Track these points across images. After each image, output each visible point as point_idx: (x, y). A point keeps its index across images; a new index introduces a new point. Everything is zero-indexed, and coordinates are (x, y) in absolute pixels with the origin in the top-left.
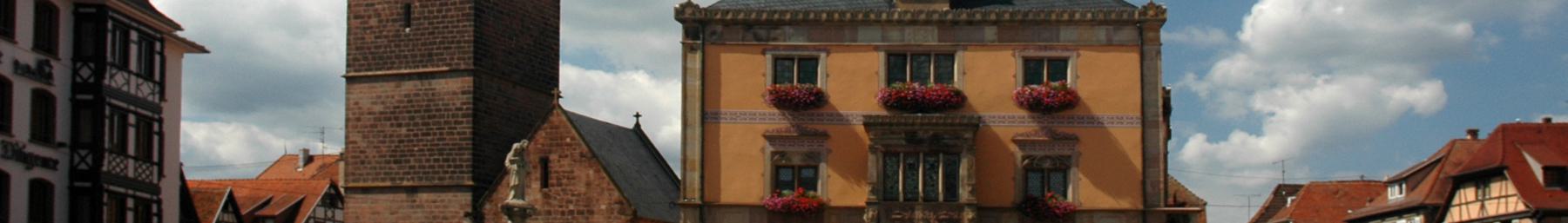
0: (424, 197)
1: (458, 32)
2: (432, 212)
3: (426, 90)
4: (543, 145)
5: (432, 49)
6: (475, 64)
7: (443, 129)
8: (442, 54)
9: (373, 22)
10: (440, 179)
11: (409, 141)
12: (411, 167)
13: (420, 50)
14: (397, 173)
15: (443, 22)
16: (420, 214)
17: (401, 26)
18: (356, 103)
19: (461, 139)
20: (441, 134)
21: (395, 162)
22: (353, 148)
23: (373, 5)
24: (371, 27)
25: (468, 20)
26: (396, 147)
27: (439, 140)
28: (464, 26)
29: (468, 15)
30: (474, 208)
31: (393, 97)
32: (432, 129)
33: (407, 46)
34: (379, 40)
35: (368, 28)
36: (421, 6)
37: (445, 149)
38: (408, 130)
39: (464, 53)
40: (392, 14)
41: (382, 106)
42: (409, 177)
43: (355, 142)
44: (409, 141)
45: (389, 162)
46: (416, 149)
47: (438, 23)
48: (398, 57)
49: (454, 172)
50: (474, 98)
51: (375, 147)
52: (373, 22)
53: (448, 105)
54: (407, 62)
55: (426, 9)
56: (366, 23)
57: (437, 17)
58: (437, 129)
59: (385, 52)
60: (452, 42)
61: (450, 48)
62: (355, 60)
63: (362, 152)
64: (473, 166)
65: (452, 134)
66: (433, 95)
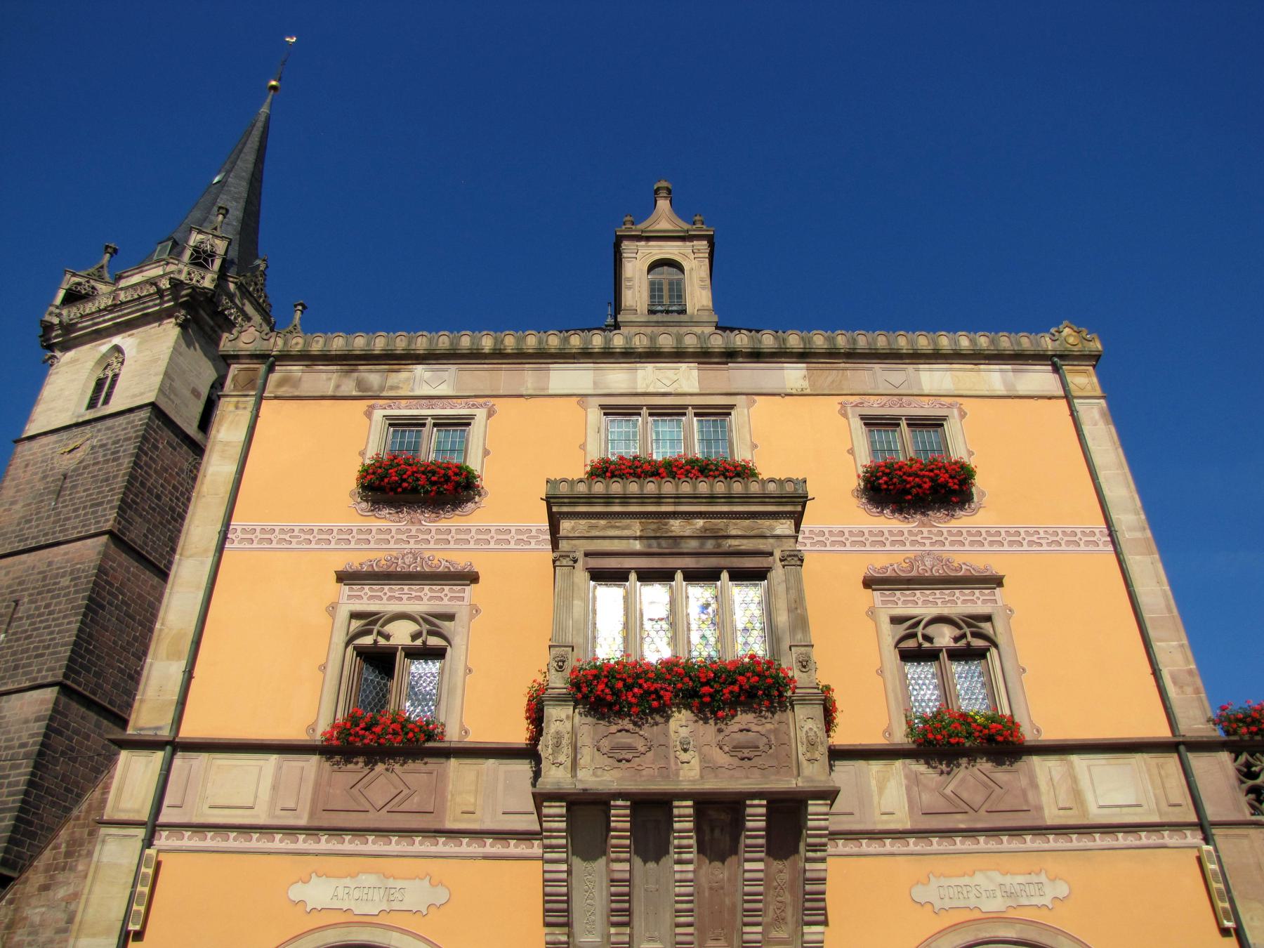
6: (66, 676)
8: (30, 665)
25: (77, 614)
28: (69, 623)
29: (79, 607)
36: (31, 602)
39: (58, 660)
50: (48, 727)
55: (33, 606)
60: (48, 647)
61: (42, 655)
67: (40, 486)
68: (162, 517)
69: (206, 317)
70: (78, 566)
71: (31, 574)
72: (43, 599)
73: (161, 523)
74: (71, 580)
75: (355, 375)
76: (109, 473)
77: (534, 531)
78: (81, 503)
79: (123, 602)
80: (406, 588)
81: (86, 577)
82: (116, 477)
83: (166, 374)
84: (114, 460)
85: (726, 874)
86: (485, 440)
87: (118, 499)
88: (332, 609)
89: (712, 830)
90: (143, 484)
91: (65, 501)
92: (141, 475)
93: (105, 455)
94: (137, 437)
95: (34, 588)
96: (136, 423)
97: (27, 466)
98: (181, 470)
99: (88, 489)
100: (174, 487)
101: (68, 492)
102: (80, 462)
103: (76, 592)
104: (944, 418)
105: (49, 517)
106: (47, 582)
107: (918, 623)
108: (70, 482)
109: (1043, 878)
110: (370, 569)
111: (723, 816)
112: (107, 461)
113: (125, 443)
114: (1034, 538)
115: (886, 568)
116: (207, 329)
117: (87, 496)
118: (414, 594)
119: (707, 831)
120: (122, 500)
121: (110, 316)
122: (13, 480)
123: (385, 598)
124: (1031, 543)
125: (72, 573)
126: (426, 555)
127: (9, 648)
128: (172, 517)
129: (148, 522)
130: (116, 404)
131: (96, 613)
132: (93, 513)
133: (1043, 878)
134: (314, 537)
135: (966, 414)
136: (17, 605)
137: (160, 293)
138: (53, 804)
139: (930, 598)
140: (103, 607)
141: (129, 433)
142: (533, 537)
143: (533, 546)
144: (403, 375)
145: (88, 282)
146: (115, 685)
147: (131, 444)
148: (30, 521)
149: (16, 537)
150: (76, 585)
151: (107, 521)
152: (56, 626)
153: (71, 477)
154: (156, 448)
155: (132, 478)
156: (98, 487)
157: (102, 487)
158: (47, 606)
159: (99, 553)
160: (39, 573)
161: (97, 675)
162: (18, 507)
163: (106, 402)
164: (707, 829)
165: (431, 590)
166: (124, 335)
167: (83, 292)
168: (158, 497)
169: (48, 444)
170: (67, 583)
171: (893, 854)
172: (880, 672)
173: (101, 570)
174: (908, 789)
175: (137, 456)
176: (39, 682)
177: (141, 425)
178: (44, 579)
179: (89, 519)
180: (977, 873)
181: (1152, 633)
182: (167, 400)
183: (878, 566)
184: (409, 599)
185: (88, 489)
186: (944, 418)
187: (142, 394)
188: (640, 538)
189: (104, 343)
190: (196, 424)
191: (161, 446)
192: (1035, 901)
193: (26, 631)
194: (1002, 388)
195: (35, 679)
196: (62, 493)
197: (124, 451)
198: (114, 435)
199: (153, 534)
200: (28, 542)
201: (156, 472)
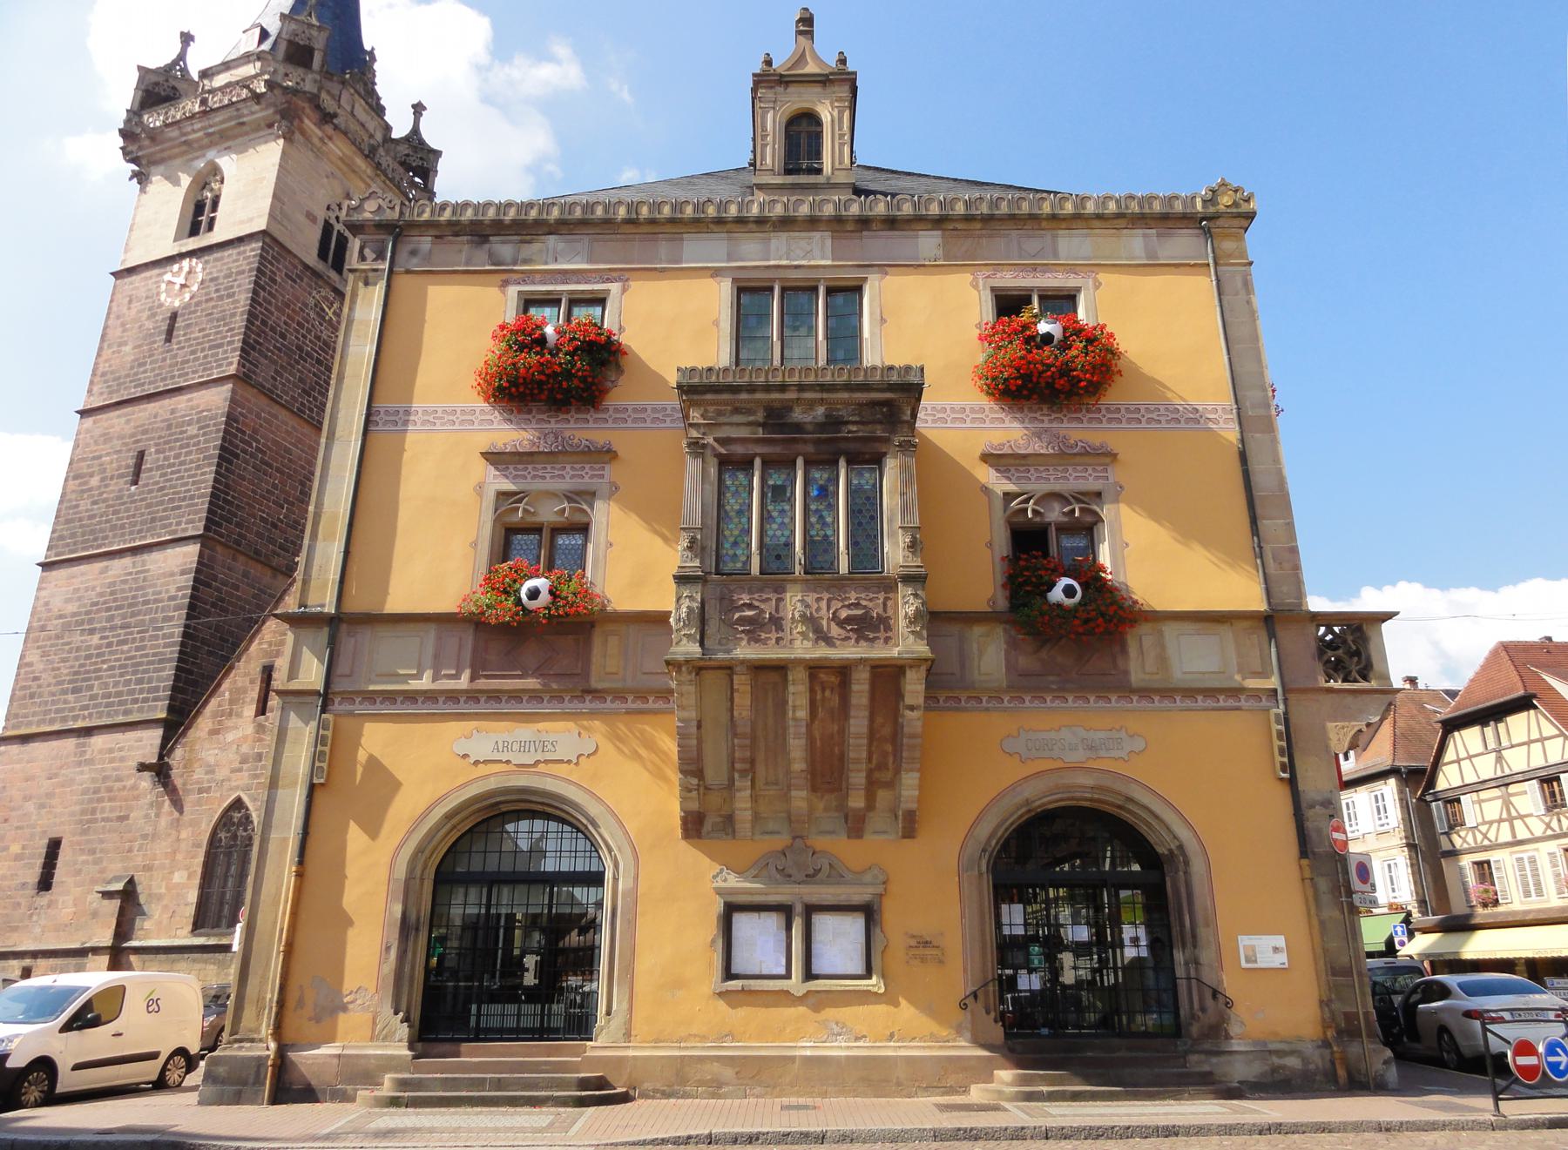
0: (98, 741)
1: (194, 483)
2: (103, 770)
3: (137, 573)
4: (270, 644)
5: (158, 511)
6: (206, 528)
7: (147, 631)
8: (167, 518)
9: (95, 481)
10: (126, 713)
11: (98, 655)
12: (92, 698)
13: (142, 515)
14: (72, 709)
15: (179, 471)
16: (84, 777)
17: (126, 483)
18: (47, 604)
19: (166, 646)
20: (142, 639)
21: (75, 691)
22: (26, 673)
23: (100, 457)
24: (90, 490)
25: (210, 465)
26: (81, 666)
27: (137, 649)
29: (210, 457)
30: (161, 757)
31: (93, 588)
32: (132, 633)
33: (127, 510)
34: (95, 507)
35: (83, 491)
36: (158, 452)
37: (140, 664)
38: (102, 638)
39: (196, 512)
40: (119, 468)
41: (78, 603)
42: (86, 713)
43: (30, 664)
44: (98, 655)
45: (64, 692)
46: (105, 666)
47: (172, 473)
48: (113, 528)
49: (145, 700)
50: (196, 580)
51: (53, 669)
52: (95, 481)
53: (160, 593)
54: (123, 535)
55: (162, 456)
56: (86, 483)
57: (170, 466)
58: (139, 632)
59: (100, 523)
60: (184, 499)
61: (179, 507)
62: (61, 538)
63: (36, 679)
64: (174, 688)
65: (156, 638)
66: (145, 579)
67: (149, 325)
68: (290, 357)
69: (313, 127)
70: (205, 414)
71: (155, 422)
72: (171, 449)
73: (289, 364)
74: (199, 429)
75: (487, 246)
76: (224, 311)
77: (669, 409)
78: (198, 344)
79: (258, 449)
80: (548, 466)
81: (215, 425)
82: (233, 315)
83: (275, 196)
84: (229, 296)
85: (836, 728)
86: (620, 316)
87: (239, 340)
88: (480, 488)
89: (823, 690)
90: (264, 323)
91: (179, 343)
92: (261, 312)
93: (217, 291)
94: (250, 270)
95: (160, 437)
96: (248, 254)
97: (130, 302)
98: (306, 305)
99: (203, 330)
100: (299, 324)
101: (182, 333)
102: (191, 298)
103: (206, 441)
104: (1078, 289)
105: (164, 360)
106: (173, 431)
107: (1030, 498)
108: (182, 321)
109: (1123, 734)
110: (514, 450)
111: (833, 679)
112: (221, 298)
113: (239, 277)
114: (1154, 416)
115: (1004, 445)
116: (316, 141)
117: (204, 337)
118: (557, 473)
119: (819, 692)
120: (244, 342)
121: (199, 126)
122: (118, 317)
123: (529, 477)
124: (1150, 420)
125: (199, 421)
126: (567, 434)
127: (142, 500)
128: (300, 357)
129: (275, 363)
130: (220, 234)
131: (230, 462)
132: (213, 355)
133: (1123, 734)
134: (457, 418)
135: (1100, 284)
136: (141, 455)
137: (257, 97)
138: (210, 653)
139: (1044, 475)
140: (237, 456)
141: (241, 265)
142: (668, 415)
143: (668, 424)
144: (536, 246)
145: (167, 81)
146: (258, 534)
147: (245, 278)
148: (144, 364)
149: (131, 382)
150: (204, 434)
151: (231, 363)
152: (189, 477)
153: (183, 315)
154: (274, 281)
155: (250, 314)
156: (215, 327)
157: (219, 326)
158: (176, 457)
159: (225, 400)
160: (163, 421)
161: (238, 525)
162: (127, 349)
163: (210, 227)
164: (818, 688)
165: (572, 468)
166: (218, 147)
167: (163, 93)
168: (283, 336)
169: (151, 277)
170: (195, 432)
171: (987, 709)
172: (990, 545)
173: (231, 418)
174: (1006, 651)
175: (255, 292)
176: (179, 535)
177: (254, 256)
178: (169, 427)
179: (210, 362)
180: (1063, 729)
181: (1259, 511)
182: (280, 226)
183: (996, 443)
184: (552, 477)
185: (203, 330)
186: (1078, 289)
187: (251, 220)
188: (764, 425)
189: (197, 158)
190: (315, 252)
191: (279, 280)
192: (1114, 754)
193: (157, 483)
194: (1143, 255)
195: (175, 532)
196: (175, 333)
197: (239, 286)
198: (225, 267)
199: (281, 376)
200: (146, 387)
201: (277, 308)
